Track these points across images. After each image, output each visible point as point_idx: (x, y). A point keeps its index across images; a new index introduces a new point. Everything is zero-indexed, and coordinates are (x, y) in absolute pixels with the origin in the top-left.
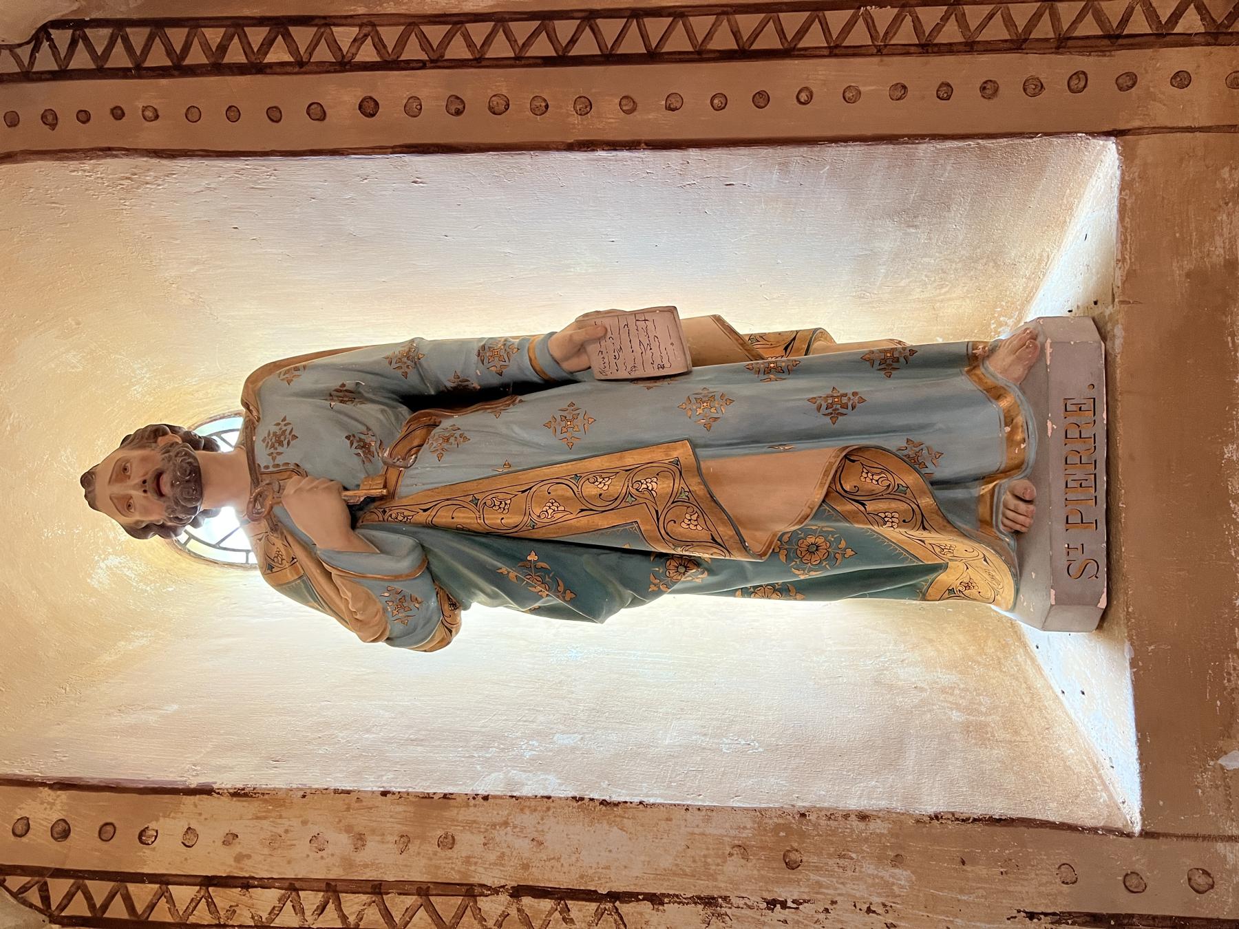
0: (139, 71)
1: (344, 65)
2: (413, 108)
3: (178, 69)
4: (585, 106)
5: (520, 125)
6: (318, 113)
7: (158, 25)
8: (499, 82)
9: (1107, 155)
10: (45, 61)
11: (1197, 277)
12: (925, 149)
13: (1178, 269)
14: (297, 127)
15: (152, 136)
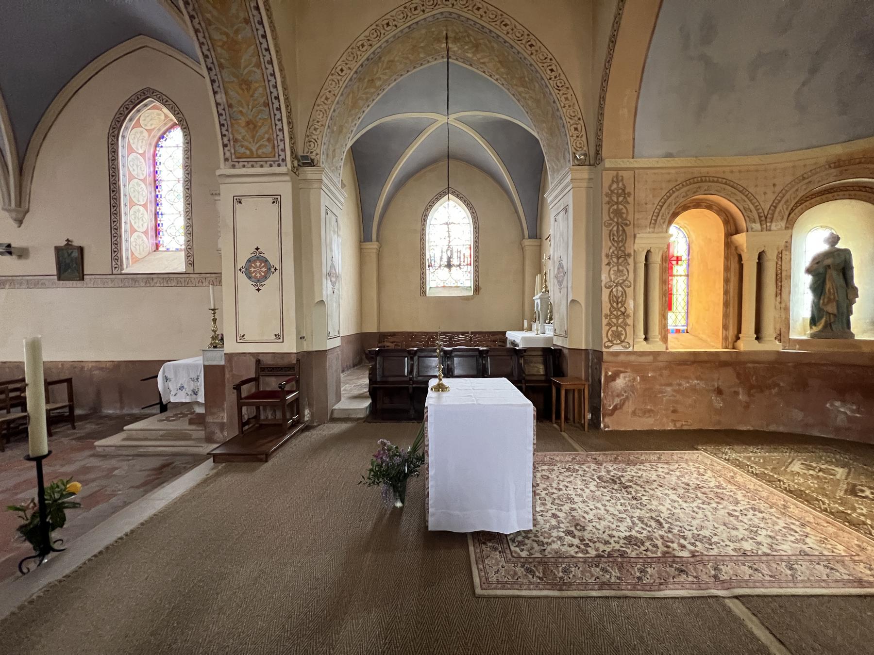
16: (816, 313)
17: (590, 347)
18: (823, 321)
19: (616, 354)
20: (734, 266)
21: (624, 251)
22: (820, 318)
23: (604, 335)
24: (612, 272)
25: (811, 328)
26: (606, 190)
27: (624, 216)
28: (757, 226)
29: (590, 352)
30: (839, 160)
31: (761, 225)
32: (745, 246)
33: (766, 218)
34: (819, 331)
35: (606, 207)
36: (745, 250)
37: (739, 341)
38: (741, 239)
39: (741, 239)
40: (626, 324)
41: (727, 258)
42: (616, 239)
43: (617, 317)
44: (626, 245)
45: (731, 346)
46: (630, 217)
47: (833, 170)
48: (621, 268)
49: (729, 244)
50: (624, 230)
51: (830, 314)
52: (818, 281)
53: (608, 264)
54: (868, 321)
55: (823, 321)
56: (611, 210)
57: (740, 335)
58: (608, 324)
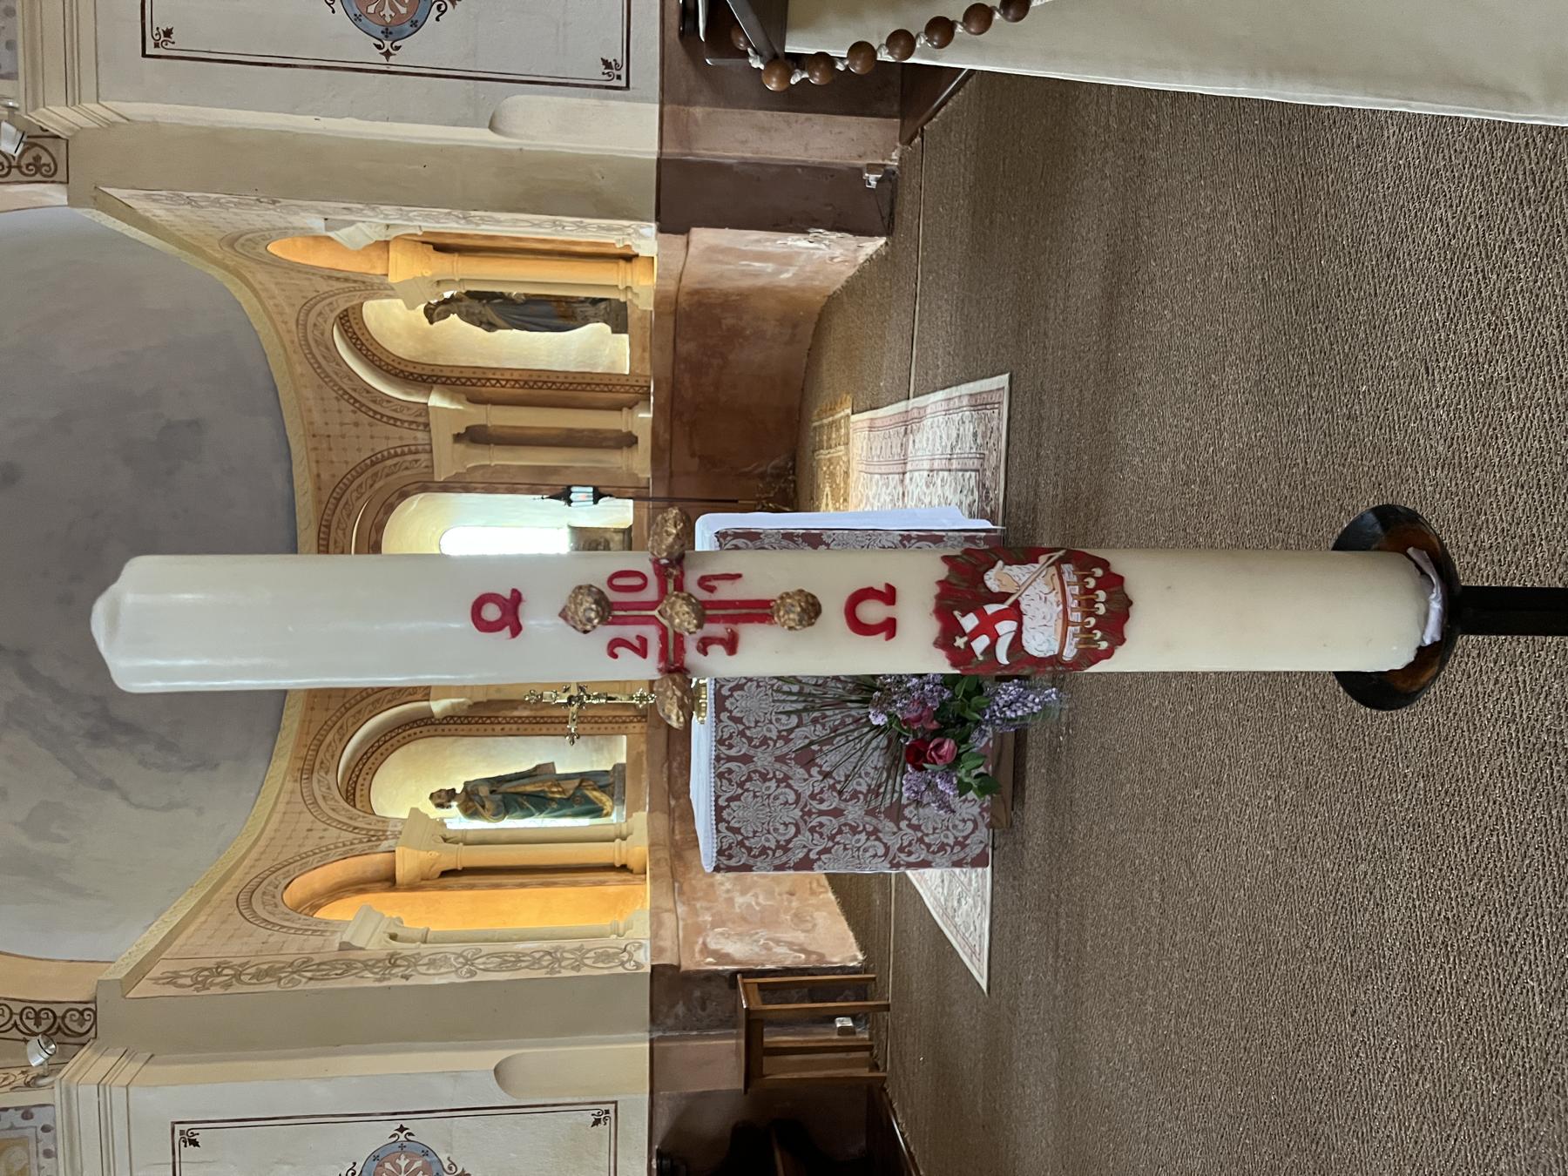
0: (462, 723)
1: (499, 723)
2: (511, 729)
3: (469, 723)
4: (540, 729)
5: (529, 732)
6: (493, 730)
7: (467, 717)
8: (526, 726)
9: (625, 737)
10: (445, 721)
11: (638, 753)
12: (597, 738)
13: (635, 752)
14: (490, 732)
15: (462, 733)
16: (577, 808)
17: (647, 1036)
18: (595, 794)
19: (657, 951)
20: (465, 880)
21: (379, 961)
22: (588, 800)
23: (606, 972)
24: (432, 971)
25: (608, 815)
26: (190, 991)
27: (278, 965)
28: (385, 845)
29: (656, 1035)
30: (302, 770)
31: (386, 839)
32: (423, 854)
33: (373, 836)
34: (612, 796)
35: (237, 988)
36: (435, 854)
37: (632, 864)
38: (408, 862)
39: (408, 862)
40: (580, 949)
41: (444, 888)
42: (339, 972)
43: (559, 961)
44: (362, 959)
45: (643, 876)
46: (290, 959)
47: (315, 775)
48: (426, 960)
49: (412, 887)
50: (319, 964)
51: (580, 785)
52: (517, 802)
53: (406, 977)
54: (594, 759)
55: (595, 794)
56: (254, 981)
57: (618, 865)
58: (577, 968)
